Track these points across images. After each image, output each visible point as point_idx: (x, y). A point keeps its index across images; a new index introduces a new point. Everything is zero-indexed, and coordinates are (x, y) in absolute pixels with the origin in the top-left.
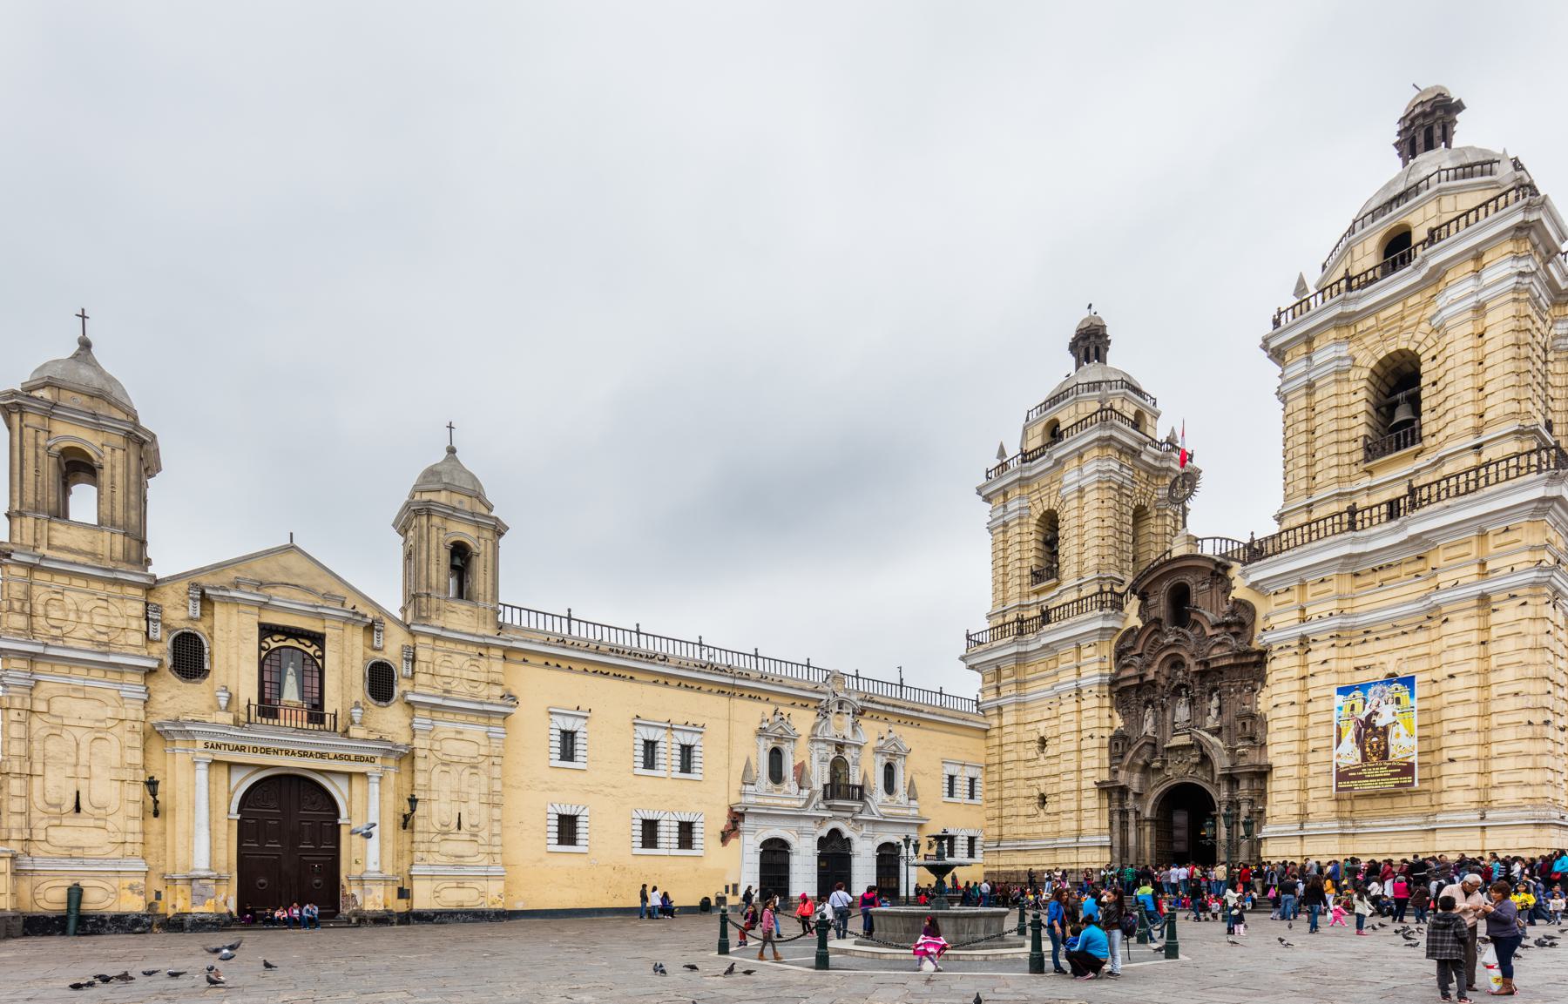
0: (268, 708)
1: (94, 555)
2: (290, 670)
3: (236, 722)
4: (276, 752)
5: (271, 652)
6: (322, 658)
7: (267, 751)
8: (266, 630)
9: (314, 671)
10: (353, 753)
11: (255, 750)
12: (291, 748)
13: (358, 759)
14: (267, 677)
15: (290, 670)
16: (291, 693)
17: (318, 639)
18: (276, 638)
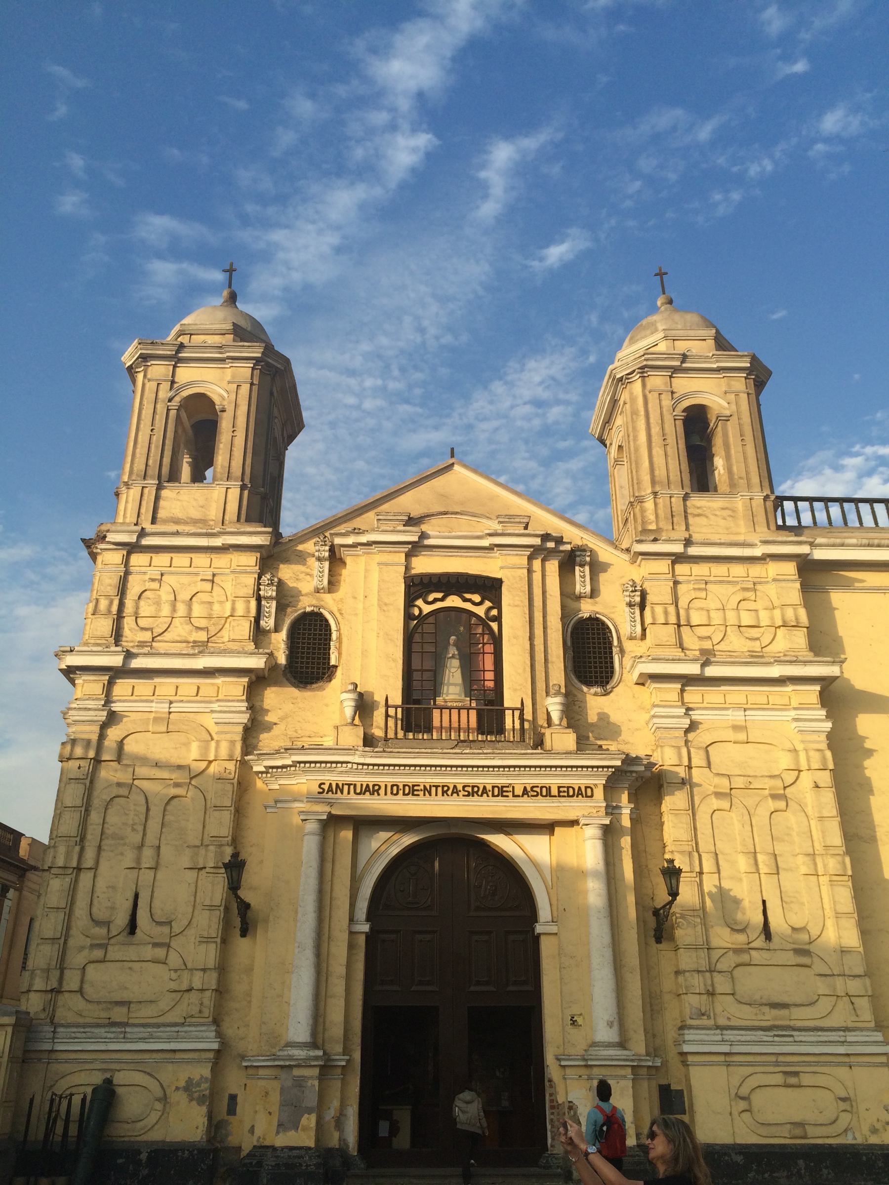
0: (416, 714)
1: (203, 521)
2: (453, 651)
3: (369, 741)
4: (427, 790)
5: (422, 618)
6: (498, 619)
7: (412, 790)
8: (417, 586)
9: (479, 641)
10: (554, 782)
11: (394, 790)
12: (450, 780)
13: (566, 792)
14: (416, 664)
15: (453, 651)
16: (453, 689)
17: (490, 588)
18: (431, 598)
